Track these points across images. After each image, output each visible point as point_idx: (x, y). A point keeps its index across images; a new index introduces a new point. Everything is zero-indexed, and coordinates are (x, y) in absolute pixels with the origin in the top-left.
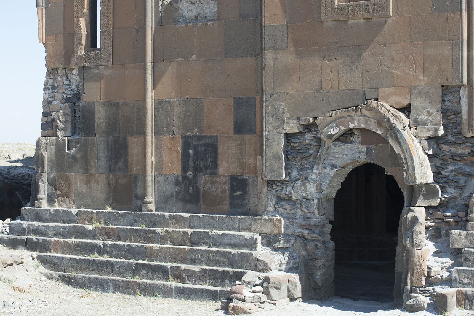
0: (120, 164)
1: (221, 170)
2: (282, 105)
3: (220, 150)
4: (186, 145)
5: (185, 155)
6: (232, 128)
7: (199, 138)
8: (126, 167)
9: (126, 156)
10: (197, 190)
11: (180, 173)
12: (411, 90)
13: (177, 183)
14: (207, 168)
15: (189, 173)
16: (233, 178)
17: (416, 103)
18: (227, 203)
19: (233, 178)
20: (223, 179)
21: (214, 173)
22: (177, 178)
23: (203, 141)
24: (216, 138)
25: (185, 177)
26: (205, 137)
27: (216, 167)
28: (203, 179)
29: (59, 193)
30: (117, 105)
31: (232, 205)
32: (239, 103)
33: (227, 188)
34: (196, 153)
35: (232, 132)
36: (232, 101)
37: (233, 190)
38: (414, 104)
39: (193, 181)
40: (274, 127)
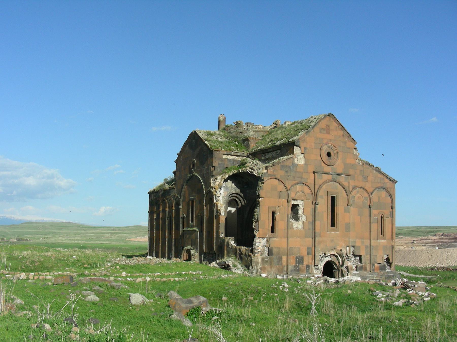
0: (280, 263)
1: (304, 263)
2: (319, 249)
3: (304, 259)
4: (297, 258)
5: (296, 261)
6: (307, 254)
7: (300, 256)
8: (282, 264)
9: (282, 261)
10: (299, 268)
11: (295, 265)
12: (342, 246)
13: (294, 267)
14: (301, 263)
15: (297, 265)
16: (307, 265)
17: (343, 249)
18: (305, 271)
19: (307, 265)
20: (305, 266)
21: (303, 264)
22: (294, 266)
23: (300, 257)
24: (303, 256)
25: (296, 265)
26: (301, 256)
27: (303, 263)
28: (300, 266)
29: (263, 271)
30: (279, 248)
31: (306, 271)
32: (308, 248)
33: (306, 268)
34: (299, 260)
35: (307, 255)
36: (307, 248)
37: (307, 268)
38: (342, 249)
39: (298, 266)
40: (318, 254)
